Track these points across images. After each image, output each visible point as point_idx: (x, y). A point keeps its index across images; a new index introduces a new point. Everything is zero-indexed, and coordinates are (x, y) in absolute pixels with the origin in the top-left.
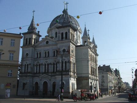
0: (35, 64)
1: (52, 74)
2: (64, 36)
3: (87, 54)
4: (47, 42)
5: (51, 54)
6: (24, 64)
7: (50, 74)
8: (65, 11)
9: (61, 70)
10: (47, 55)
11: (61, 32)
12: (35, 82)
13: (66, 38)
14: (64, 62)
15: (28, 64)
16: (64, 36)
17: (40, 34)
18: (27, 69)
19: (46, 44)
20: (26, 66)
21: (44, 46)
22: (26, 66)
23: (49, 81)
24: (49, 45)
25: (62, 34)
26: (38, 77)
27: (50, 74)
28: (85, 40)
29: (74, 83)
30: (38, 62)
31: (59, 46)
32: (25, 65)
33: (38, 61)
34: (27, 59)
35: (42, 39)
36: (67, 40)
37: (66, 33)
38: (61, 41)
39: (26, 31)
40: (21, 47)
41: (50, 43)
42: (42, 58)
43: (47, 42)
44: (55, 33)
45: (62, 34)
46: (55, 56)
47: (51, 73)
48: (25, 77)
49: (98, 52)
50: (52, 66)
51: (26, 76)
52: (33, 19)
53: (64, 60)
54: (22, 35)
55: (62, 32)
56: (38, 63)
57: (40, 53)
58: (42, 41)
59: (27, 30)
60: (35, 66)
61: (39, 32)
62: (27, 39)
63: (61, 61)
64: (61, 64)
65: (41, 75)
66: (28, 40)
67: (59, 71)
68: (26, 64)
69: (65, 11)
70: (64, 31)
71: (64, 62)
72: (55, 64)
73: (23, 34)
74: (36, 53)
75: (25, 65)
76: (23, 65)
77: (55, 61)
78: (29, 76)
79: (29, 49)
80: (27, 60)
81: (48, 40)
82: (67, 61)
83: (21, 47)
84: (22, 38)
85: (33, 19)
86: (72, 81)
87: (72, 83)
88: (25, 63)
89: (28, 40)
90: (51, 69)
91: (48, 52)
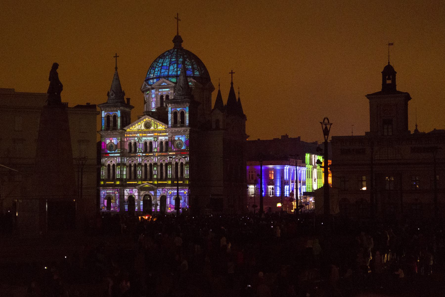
6: (107, 165)
10: (148, 148)
17: (131, 103)
46: (164, 150)
56: (133, 161)
61: (128, 99)
68: (111, 165)
72: (164, 164)
88: (109, 162)
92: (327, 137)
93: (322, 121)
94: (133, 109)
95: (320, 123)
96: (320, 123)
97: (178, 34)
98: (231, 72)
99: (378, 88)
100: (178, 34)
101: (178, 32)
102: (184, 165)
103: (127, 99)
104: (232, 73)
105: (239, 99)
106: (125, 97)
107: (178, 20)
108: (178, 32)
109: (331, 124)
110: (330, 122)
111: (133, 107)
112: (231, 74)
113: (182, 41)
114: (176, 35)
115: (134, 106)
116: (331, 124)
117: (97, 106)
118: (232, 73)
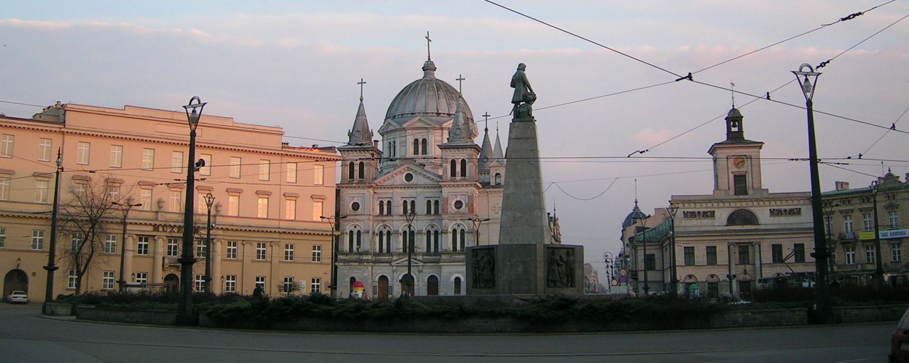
1: (425, 257)
2: (458, 168)
4: (409, 177)
5: (421, 208)
6: (348, 232)
7: (420, 258)
8: (429, 68)
9: (451, 249)
11: (450, 158)
13: (463, 173)
14: (459, 231)
15: (359, 232)
16: (458, 168)
18: (359, 243)
19: (406, 182)
20: (355, 237)
22: (355, 237)
23: (417, 273)
24: (416, 187)
25: (453, 163)
26: (388, 264)
27: (420, 258)
28: (498, 172)
31: (446, 192)
32: (351, 232)
33: (385, 223)
34: (357, 217)
36: (465, 180)
37: (463, 163)
38: (453, 183)
41: (417, 179)
42: (395, 218)
44: (413, 141)
45: (453, 163)
47: (424, 254)
48: (357, 264)
50: (425, 237)
51: (361, 262)
52: (361, 105)
53: (459, 226)
55: (453, 158)
57: (389, 203)
59: (347, 139)
63: (450, 230)
64: (450, 236)
65: (395, 258)
66: (357, 168)
67: (446, 252)
68: (355, 232)
69: (429, 68)
70: (459, 155)
71: (459, 231)
72: (432, 232)
75: (351, 232)
76: (346, 233)
77: (432, 227)
78: (368, 261)
79: (362, 191)
80: (357, 220)
82: (466, 230)
85: (361, 105)
88: (352, 228)
89: (357, 168)
91: (413, 203)
97: (429, 59)
98: (488, 115)
99: (723, 138)
100: (429, 59)
101: (429, 57)
102: (466, 232)
103: (374, 141)
107: (429, 40)
118: (486, 116)
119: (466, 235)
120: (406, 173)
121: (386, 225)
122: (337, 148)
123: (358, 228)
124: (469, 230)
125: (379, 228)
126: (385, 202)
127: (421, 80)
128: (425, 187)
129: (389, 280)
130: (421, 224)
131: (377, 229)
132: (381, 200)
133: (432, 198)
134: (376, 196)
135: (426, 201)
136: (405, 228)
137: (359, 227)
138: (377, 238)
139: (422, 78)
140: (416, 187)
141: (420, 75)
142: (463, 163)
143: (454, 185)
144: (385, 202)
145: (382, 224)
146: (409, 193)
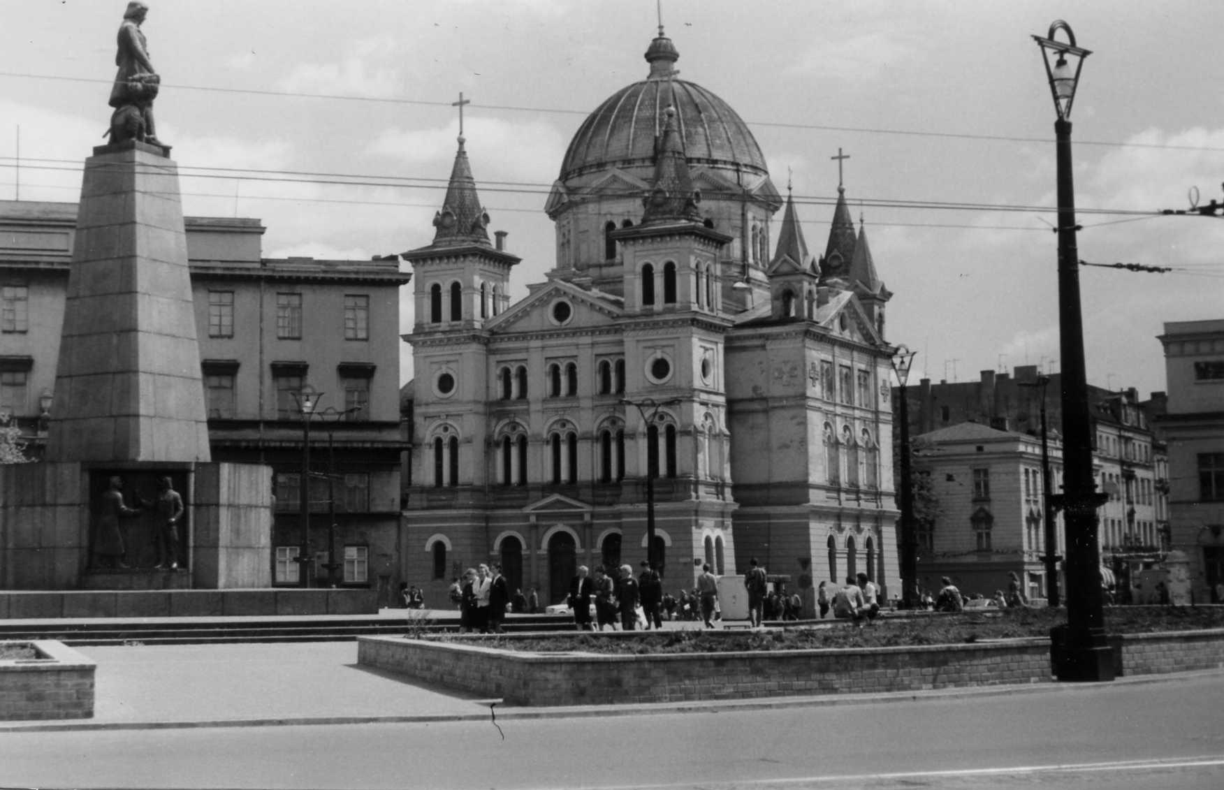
0: (496, 437)
3: (797, 370)
4: (562, 312)
5: (588, 381)
8: (660, 54)
12: (504, 534)
14: (662, 429)
17: (509, 248)
19: (555, 322)
21: (542, 335)
24: (577, 331)
25: (648, 271)
29: (718, 540)
30: (514, 426)
35: (527, 293)
36: (672, 311)
39: (424, 235)
40: (407, 338)
41: (578, 316)
43: (562, 312)
45: (648, 271)
46: (613, 390)
49: (892, 335)
53: (662, 418)
54: (405, 267)
58: (533, 306)
60: (497, 444)
61: (500, 235)
62: (436, 289)
64: (643, 444)
68: (446, 441)
69: (660, 54)
71: (662, 429)
73: (413, 257)
74: (498, 372)
75: (439, 442)
81: (565, 300)
83: (407, 338)
84: (406, 282)
86: (706, 532)
87: (708, 540)
90: (589, 465)
91: (572, 369)
92: (1069, 107)
93: (1045, 35)
94: (514, 267)
95: (1037, 38)
96: (1037, 38)
97: (661, 34)
100: (661, 34)
104: (840, 157)
105: (862, 232)
106: (491, 230)
108: (661, 27)
109: (1085, 54)
110: (1079, 44)
111: (516, 261)
112: (837, 161)
113: (674, 57)
114: (657, 36)
115: (519, 256)
116: (1085, 54)
117: (400, 259)
118: (840, 157)
119: (678, 441)
120: (555, 302)
121: (515, 422)
122: (409, 256)
123: (451, 432)
124: (682, 426)
125: (502, 428)
126: (513, 371)
127: (642, 83)
128: (594, 330)
129: (524, 546)
130: (586, 421)
131: (497, 430)
132: (503, 365)
133: (612, 357)
134: (493, 359)
135: (548, 368)
136: (555, 427)
137: (453, 430)
138: (499, 455)
139: (644, 78)
140: (577, 331)
141: (642, 71)
142: (670, 270)
143: (646, 324)
144: (513, 371)
145: (507, 421)
146: (560, 348)
